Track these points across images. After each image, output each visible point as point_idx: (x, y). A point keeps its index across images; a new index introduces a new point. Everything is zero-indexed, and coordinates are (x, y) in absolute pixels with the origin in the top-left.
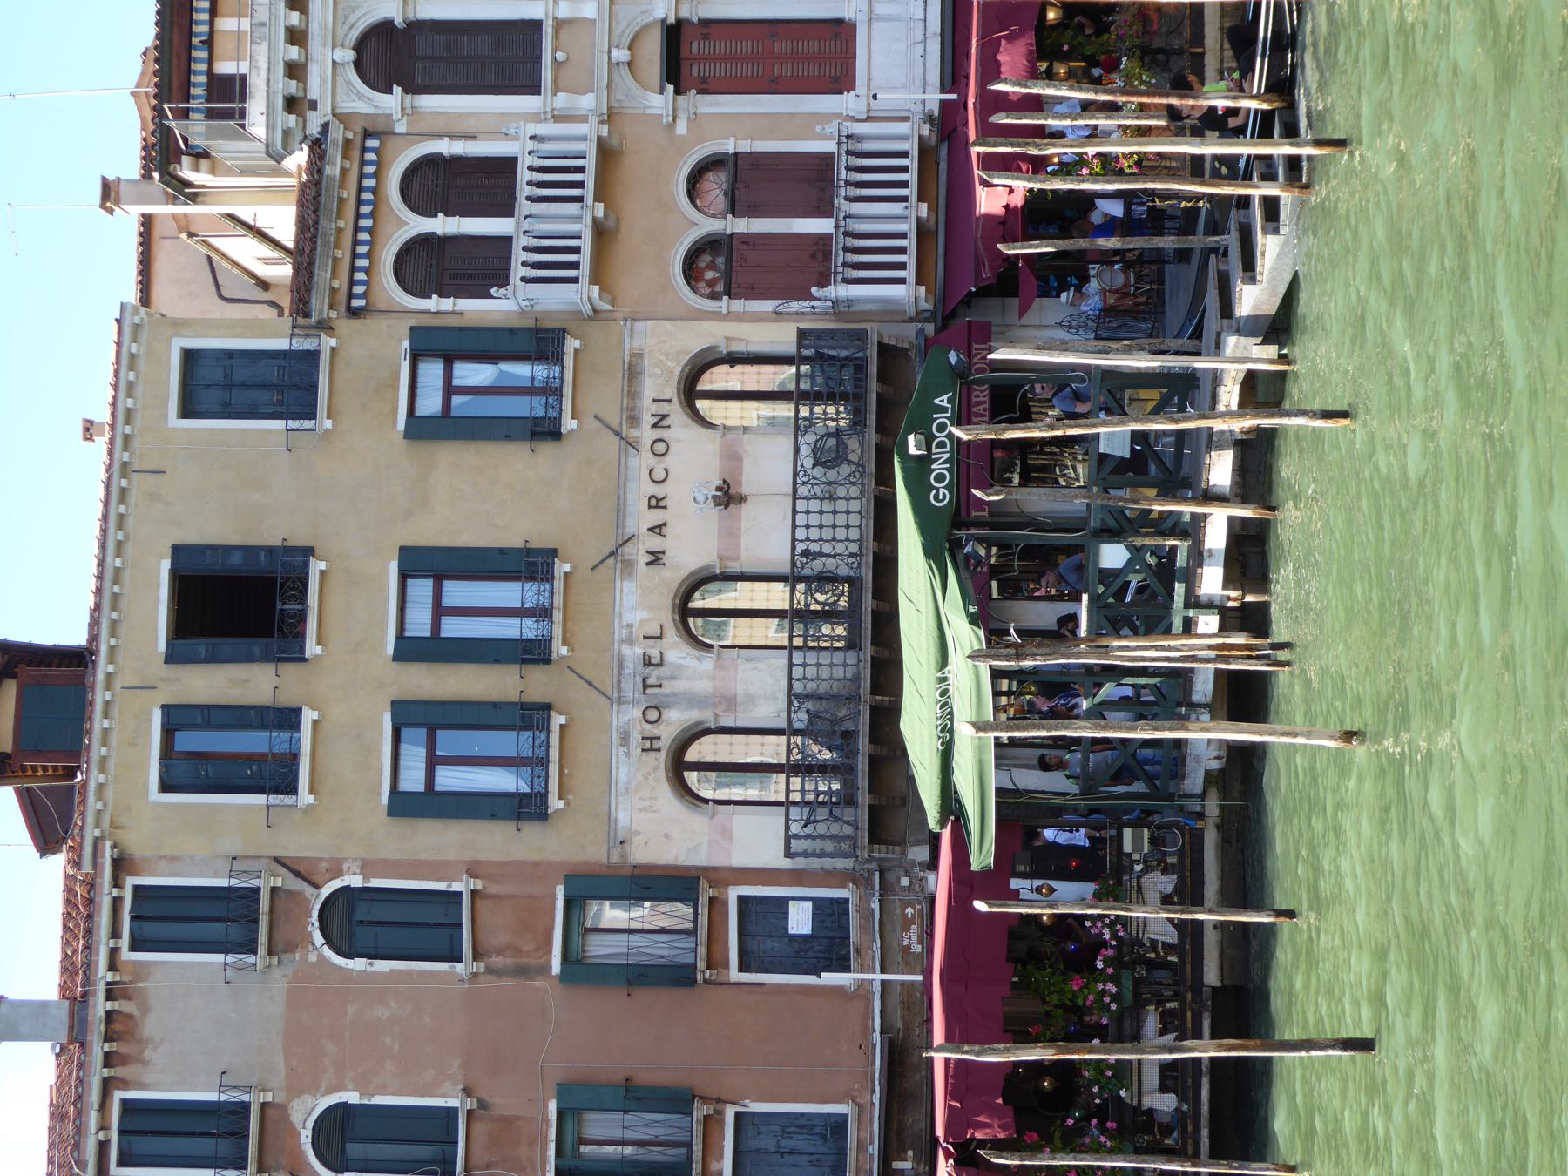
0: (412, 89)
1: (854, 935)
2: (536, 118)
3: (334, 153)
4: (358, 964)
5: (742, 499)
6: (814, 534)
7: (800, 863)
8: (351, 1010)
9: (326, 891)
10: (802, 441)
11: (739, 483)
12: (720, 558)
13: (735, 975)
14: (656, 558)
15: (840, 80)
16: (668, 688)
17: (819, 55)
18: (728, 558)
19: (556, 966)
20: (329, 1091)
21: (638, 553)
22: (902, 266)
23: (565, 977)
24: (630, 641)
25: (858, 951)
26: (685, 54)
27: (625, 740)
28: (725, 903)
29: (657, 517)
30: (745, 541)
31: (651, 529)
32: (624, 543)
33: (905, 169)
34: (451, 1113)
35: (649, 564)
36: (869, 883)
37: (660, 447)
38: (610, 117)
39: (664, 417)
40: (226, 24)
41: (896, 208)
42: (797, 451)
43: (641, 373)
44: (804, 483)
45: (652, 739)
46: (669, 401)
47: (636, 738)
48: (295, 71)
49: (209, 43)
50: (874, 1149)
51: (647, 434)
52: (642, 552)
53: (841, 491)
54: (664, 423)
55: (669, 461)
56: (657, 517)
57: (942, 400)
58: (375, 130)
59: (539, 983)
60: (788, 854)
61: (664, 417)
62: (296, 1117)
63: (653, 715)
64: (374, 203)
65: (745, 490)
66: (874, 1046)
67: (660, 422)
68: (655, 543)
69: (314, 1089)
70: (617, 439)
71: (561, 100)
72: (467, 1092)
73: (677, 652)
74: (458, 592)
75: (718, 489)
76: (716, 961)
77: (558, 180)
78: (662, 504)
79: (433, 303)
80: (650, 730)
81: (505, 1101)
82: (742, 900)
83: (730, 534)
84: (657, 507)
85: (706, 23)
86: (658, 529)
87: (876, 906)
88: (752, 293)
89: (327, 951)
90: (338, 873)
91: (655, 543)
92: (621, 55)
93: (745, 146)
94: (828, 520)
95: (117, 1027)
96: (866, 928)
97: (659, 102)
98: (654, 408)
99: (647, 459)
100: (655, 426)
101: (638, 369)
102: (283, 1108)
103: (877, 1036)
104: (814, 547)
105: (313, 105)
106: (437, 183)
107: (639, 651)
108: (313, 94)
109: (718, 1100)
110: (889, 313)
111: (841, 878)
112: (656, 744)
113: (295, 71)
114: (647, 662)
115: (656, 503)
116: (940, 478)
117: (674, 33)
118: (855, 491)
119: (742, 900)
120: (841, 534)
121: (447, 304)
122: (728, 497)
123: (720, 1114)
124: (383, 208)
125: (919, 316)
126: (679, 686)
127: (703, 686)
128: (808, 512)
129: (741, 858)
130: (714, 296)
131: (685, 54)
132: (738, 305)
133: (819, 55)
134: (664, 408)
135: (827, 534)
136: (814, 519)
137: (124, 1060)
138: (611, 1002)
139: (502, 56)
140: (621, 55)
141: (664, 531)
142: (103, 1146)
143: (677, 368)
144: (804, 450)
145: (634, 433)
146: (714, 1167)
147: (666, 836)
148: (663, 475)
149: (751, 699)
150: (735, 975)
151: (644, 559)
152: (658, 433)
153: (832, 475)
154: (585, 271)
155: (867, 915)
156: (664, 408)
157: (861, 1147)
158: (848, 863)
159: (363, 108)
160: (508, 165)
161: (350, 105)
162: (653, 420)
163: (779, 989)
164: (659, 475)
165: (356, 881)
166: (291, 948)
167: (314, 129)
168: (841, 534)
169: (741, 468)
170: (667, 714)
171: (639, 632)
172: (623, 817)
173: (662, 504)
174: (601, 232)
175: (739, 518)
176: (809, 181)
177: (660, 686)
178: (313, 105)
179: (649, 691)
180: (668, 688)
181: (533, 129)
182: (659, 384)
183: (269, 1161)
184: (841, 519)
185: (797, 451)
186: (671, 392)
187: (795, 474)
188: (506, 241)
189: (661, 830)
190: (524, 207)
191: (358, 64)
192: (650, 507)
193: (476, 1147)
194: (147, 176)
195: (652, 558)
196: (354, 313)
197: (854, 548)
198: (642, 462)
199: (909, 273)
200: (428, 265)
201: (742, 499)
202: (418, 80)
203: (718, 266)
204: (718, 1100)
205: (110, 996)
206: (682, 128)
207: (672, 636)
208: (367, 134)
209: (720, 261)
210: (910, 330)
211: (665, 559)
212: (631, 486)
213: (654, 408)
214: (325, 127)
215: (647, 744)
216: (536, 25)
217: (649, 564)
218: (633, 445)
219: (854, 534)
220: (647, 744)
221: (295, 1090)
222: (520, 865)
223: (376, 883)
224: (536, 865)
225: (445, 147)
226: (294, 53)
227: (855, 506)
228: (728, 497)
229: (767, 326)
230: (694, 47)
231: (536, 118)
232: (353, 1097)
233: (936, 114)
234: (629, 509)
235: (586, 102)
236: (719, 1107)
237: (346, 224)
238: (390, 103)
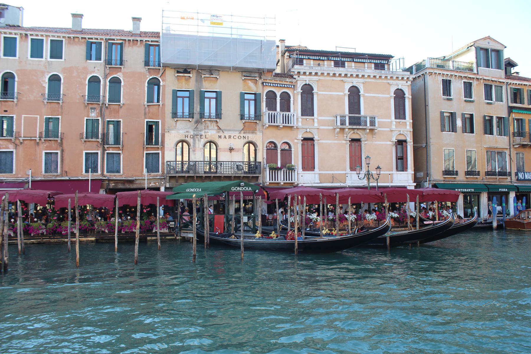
0: (302, 94)
2: (297, 115)
3: (291, 80)
4: (146, 85)
5: (231, 152)
6: (225, 165)
7: (166, 164)
8: (138, 83)
9: (159, 79)
13: (145, 152)
14: (220, 137)
15: (304, 169)
17: (309, 165)
20: (124, 80)
24: (205, 132)
26: (308, 141)
27: (187, 132)
29: (227, 137)
34: (120, 101)
36: (162, 176)
37: (240, 137)
38: (297, 128)
40: (312, 62)
41: (282, 179)
47: (187, 134)
48: (305, 73)
49: (309, 59)
50: (114, 178)
51: (242, 135)
53: (232, 170)
56: (227, 137)
57: (250, 189)
58: (295, 87)
60: (167, 162)
62: (119, 74)
63: (192, 137)
64: (282, 87)
67: (244, 137)
68: (223, 137)
69: (124, 77)
71: (300, 120)
72: (123, 104)
73: (203, 141)
74: (213, 102)
77: (286, 119)
79: (265, 97)
80: (189, 136)
81: (122, 111)
83: (225, 150)
85: (314, 145)
86: (225, 137)
88: (267, 154)
89: (149, 79)
90: (163, 81)
92: (308, 130)
93: (293, 152)
94: (227, 168)
95: (135, 42)
97: (300, 137)
102: (120, 71)
105: (299, 77)
106: (286, 98)
108: (301, 77)
110: (264, 178)
111: (163, 172)
113: (305, 73)
114: (201, 136)
115: (230, 137)
116: (236, 189)
117: (312, 139)
118: (232, 172)
120: (225, 170)
121: (265, 100)
122: (231, 150)
123: (120, 150)
124: (281, 88)
125: (264, 183)
126: (197, 141)
127: (197, 145)
130: (267, 147)
131: (308, 141)
132: (265, 151)
133: (309, 165)
134: (247, 138)
135: (225, 168)
136: (227, 165)
137: (129, 43)
139: (308, 110)
140: (308, 130)
142: (114, 40)
143: (254, 140)
144: (240, 163)
146: (111, 149)
149: (195, 154)
150: (145, 152)
153: (235, 168)
154: (271, 124)
155: (157, 176)
156: (247, 138)
157: (115, 176)
158: (166, 172)
159: (298, 85)
160: (289, 110)
161: (298, 82)
163: (143, 160)
165: (161, 84)
166: (149, 72)
167: (295, 77)
168: (225, 170)
172: (173, 132)
174: (278, 126)
178: (299, 77)
180: (197, 139)
181: (295, 115)
182: (251, 137)
183: (111, 69)
184: (227, 170)
186: (250, 139)
188: (276, 110)
189: (170, 139)
190: (282, 113)
191: (306, 84)
193: (113, 106)
194: (286, 47)
196: (263, 83)
198: (237, 134)
199: (271, 181)
200: (271, 96)
201: (231, 152)
202: (303, 95)
203: (272, 148)
205: (141, 40)
206: (296, 141)
207: (206, 140)
208: (294, 86)
209: (273, 148)
210: (261, 182)
214: (295, 79)
216: (313, 115)
218: (240, 133)
219: (225, 172)
221: (124, 74)
222: (164, 113)
223: (161, 87)
224: (165, 116)
225: (292, 100)
226: (308, 73)
227: (230, 172)
228: (231, 150)
229: (262, 157)
230: (310, 143)
231: (297, 115)
232: (122, 84)
235: (300, 124)
237: (278, 82)
238: (299, 90)
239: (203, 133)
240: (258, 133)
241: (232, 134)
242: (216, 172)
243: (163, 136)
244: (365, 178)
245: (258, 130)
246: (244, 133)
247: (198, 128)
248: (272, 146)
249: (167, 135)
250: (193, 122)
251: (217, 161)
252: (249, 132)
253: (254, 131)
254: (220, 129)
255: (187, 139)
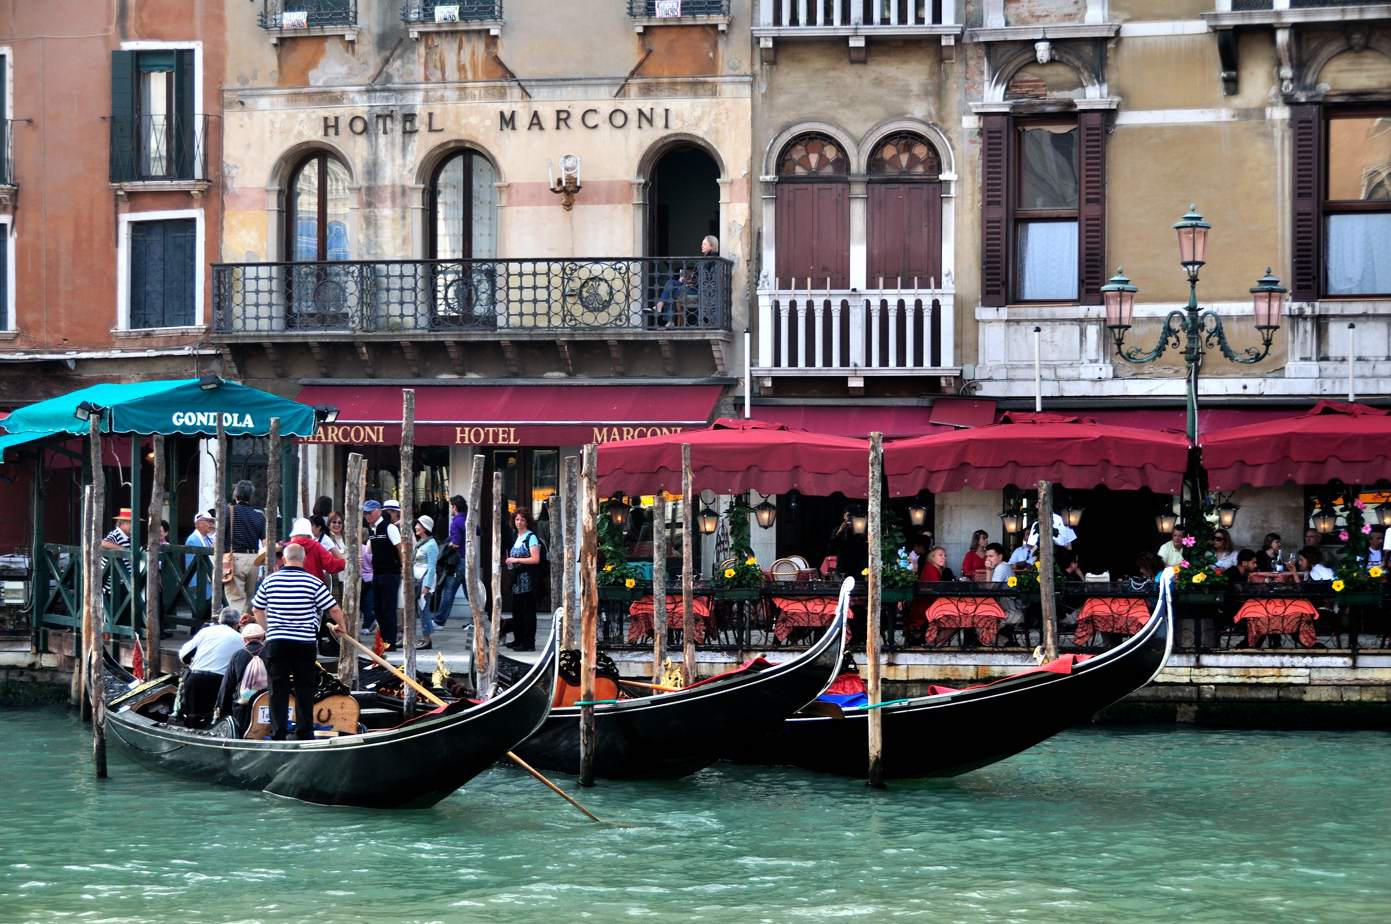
1: (159, 330)
5: (568, 206)
10: (605, 265)
11: (585, 201)
12: (509, 186)
13: (126, 218)
14: (508, 121)
16: (382, 139)
18: (510, 196)
19: (128, 46)
21: (514, 104)
22: (793, 362)
23: (118, 56)
24: (426, 100)
25: (148, 335)
28: (188, 206)
29: (549, 119)
30: (528, 210)
31: (536, 114)
32: (523, 89)
33: (810, 362)
35: (502, 114)
39: (650, 121)
42: (597, 260)
43: (696, 95)
44: (564, 269)
45: (336, 127)
46: (667, 126)
51: (632, 104)
52: (515, 107)
54: (644, 121)
55: (605, 128)
56: (549, 119)
57: (249, 421)
59: (113, 29)
61: (650, 121)
63: (359, 126)
65: (577, 208)
66: (63, 353)
68: (523, 120)
70: (627, 75)
75: (571, 180)
76: (135, 199)
78: (562, 124)
80: (343, 124)
82: (192, 222)
83: (533, 195)
84: (559, 120)
86: (536, 121)
87: (186, 351)
91: (523, 120)
94: (528, 294)
96: (169, 342)
98: (659, 112)
99: (606, 107)
100: (641, 112)
101: (701, 91)
103: (73, 355)
104: (500, 282)
107: (420, 110)
109: (15, 208)
112: (331, 131)
115: (562, 118)
118: (556, 321)
119: (192, 222)
122: (569, 192)
128: (535, 274)
129: (231, 219)
134: (659, 122)
135: (542, 294)
136: (528, 281)
138: (99, 104)
141: (535, 128)
143: (702, 131)
144: (597, 269)
145: (633, 90)
147: (249, 146)
148: (591, 124)
150: (126, 218)
151: (507, 109)
152: (633, 117)
155: (181, 340)
156: (659, 122)
162: (647, 111)
164: (591, 120)
168: (515, 308)
169: (598, 203)
170: (361, 141)
171: (437, 109)
172: (264, 103)
173: (562, 124)
175: (549, 204)
176: (907, 260)
177: (385, 132)
179: (381, 122)
180: (382, 139)
182: (687, 115)
184: (528, 308)
185: (597, 260)
186: (677, 127)
187: (572, 260)
192: (558, 112)
195: (508, 115)
197: (501, 321)
199: (785, 369)
201: (568, 206)
204: (15, 208)
207: (435, 140)
209: (828, 170)
211: (507, 131)
212: (579, 92)
213: (659, 112)
215: (332, 122)
217: (502, 114)
218: (622, 92)
220: (332, 122)
227: (542, 322)
228: (569, 192)
233: (978, 393)
234: (558, 92)
236: (10, 208)
239: (416, 101)
240: (727, 90)
241: (576, 101)
242: (490, 321)
243: (214, 128)
244: (1171, 353)
245: (723, 66)
246: (647, 90)
247: (389, 79)
248: (914, 160)
249: (232, 120)
250: (366, 47)
251: (467, 259)
252: (673, 88)
253: (700, 82)
254: (509, 75)
255: (333, 141)
